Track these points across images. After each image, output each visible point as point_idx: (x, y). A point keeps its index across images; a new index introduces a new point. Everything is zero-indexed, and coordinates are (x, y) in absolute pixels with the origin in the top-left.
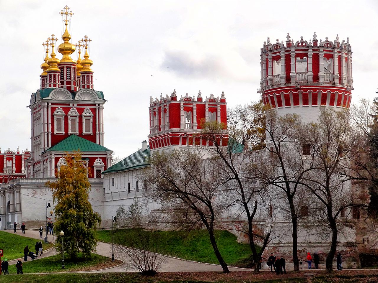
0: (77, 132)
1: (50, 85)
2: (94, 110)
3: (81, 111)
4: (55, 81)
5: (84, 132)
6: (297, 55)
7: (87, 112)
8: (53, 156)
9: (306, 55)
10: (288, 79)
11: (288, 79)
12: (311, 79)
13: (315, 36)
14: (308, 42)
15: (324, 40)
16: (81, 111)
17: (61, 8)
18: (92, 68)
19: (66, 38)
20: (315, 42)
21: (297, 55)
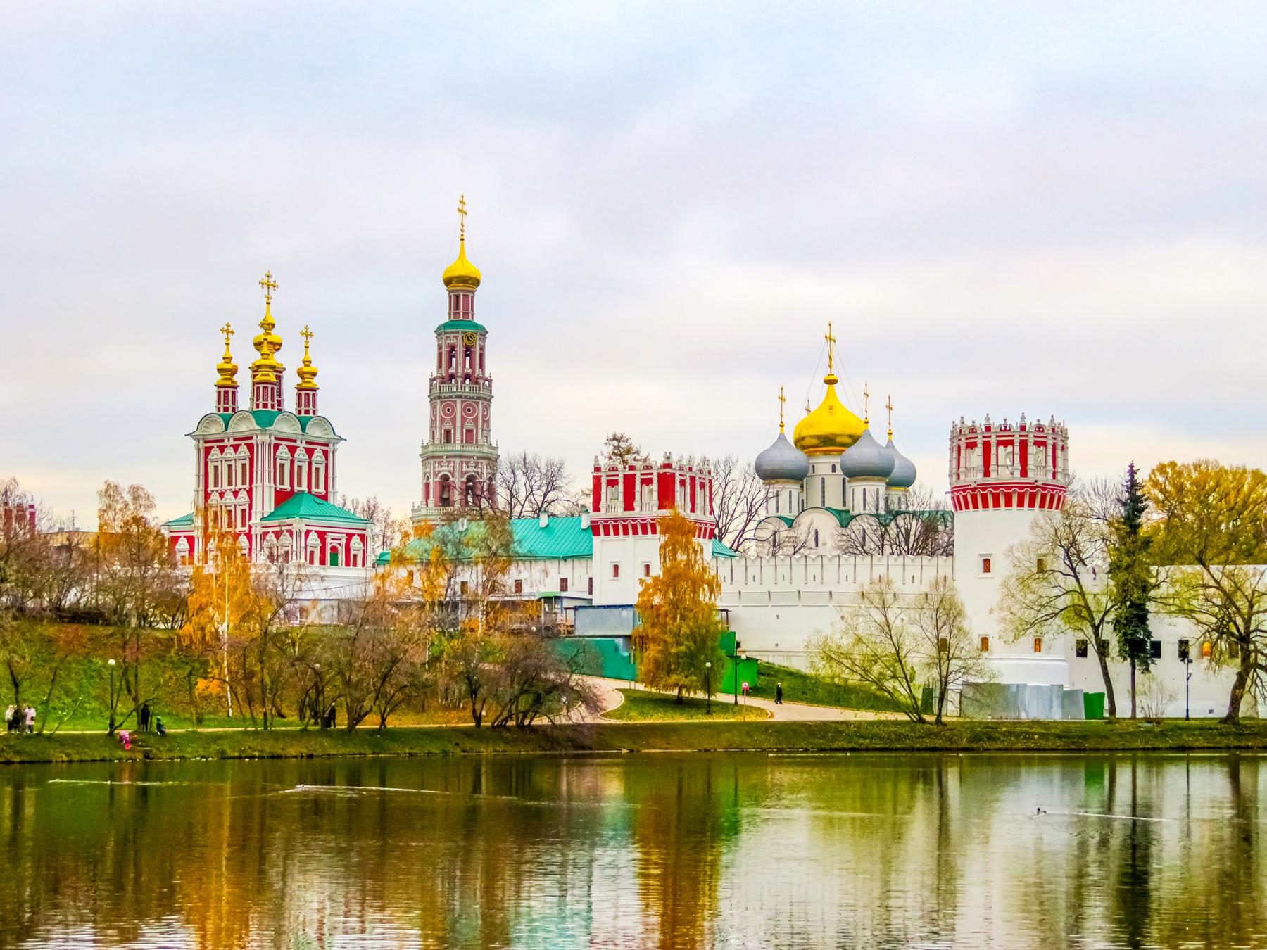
0: (304, 488)
1: (265, 406)
2: (325, 453)
3: (310, 452)
4: (265, 398)
5: (314, 490)
6: (999, 443)
7: (318, 456)
8: (304, 529)
9: (1011, 443)
10: (987, 474)
11: (987, 474)
12: (1017, 474)
13: (1023, 418)
14: (1014, 426)
15: (1035, 423)
16: (310, 452)
17: (261, 276)
18: (316, 382)
19: (268, 326)
20: (1023, 428)
21: (999, 443)
